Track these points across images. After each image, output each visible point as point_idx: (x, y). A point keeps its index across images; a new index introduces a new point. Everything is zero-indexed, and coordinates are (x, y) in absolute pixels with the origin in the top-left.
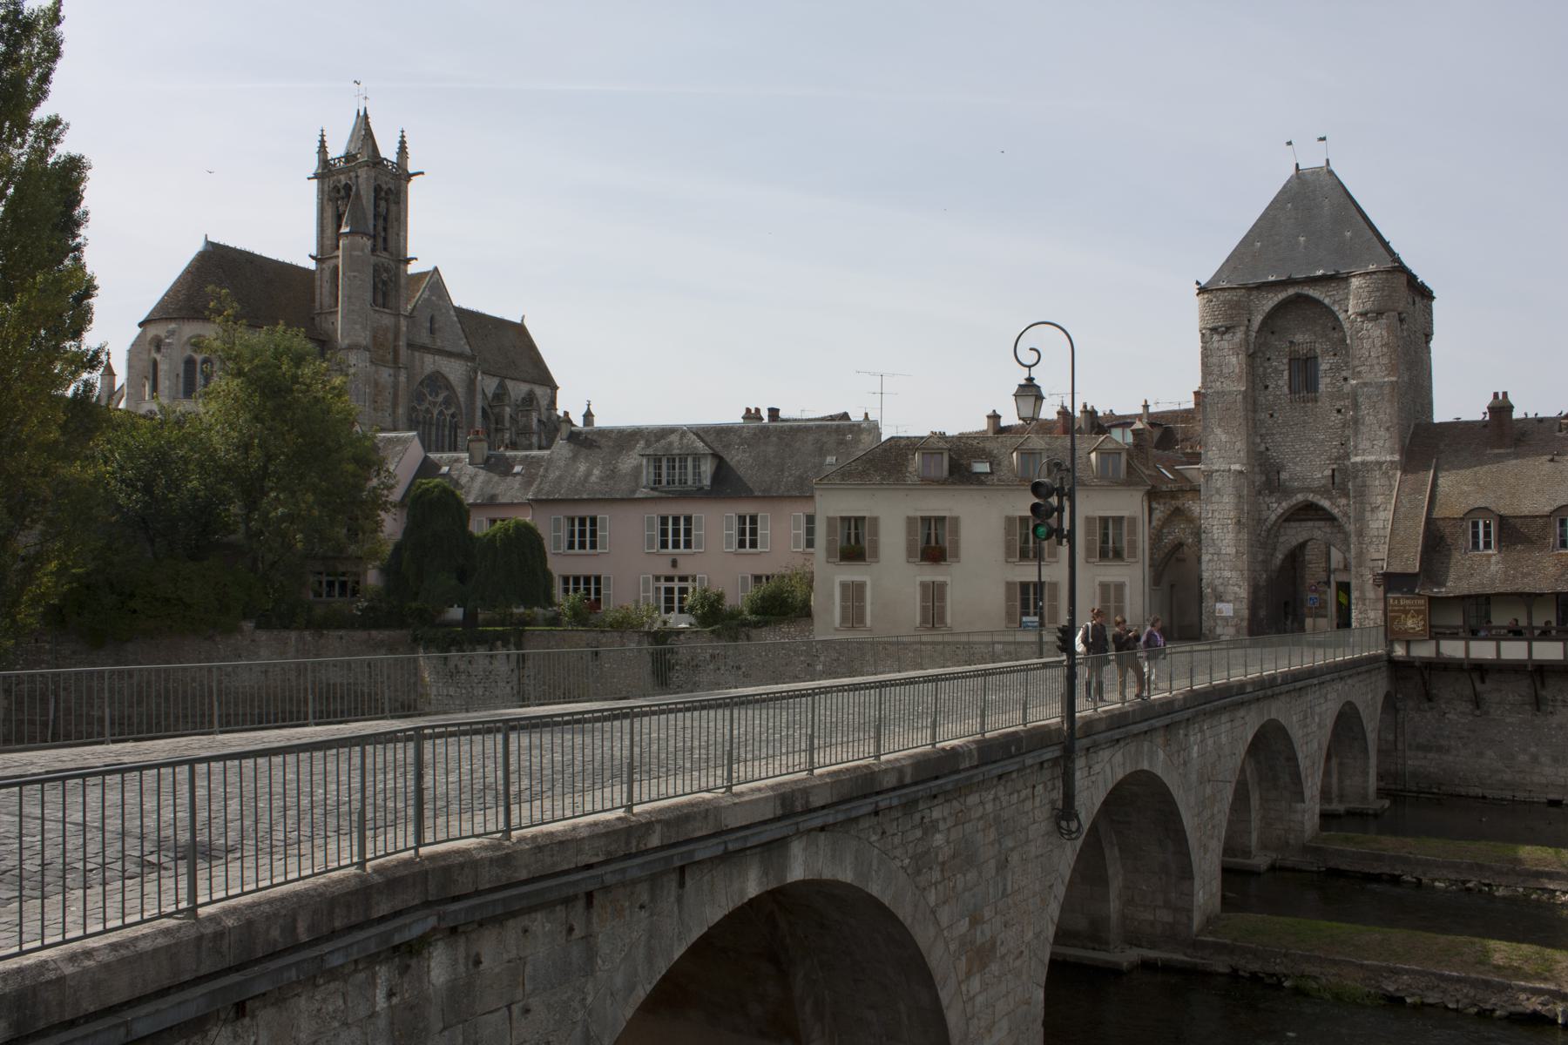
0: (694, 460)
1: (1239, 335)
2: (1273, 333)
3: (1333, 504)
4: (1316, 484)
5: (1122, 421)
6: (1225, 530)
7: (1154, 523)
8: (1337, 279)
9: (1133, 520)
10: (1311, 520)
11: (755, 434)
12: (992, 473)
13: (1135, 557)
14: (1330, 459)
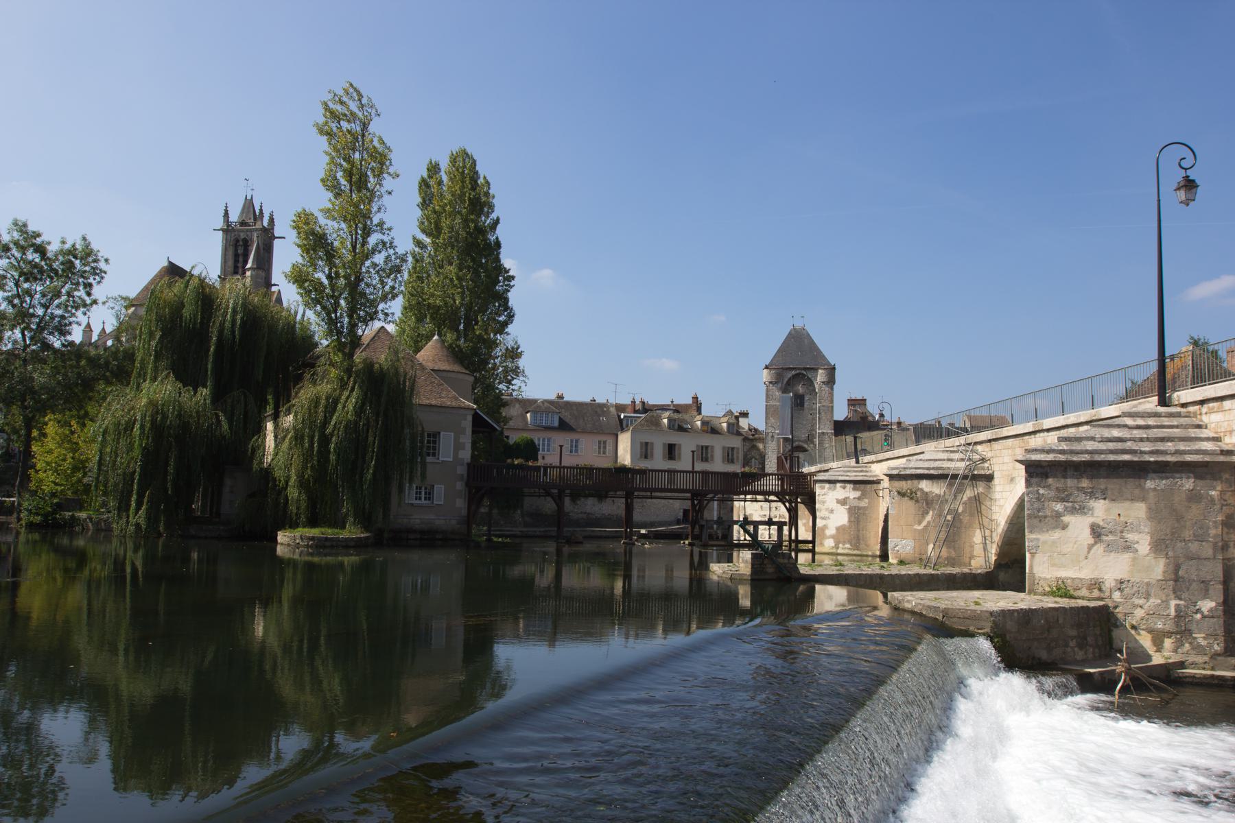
1: (780, 385)
8: (816, 370)
9: (738, 449)
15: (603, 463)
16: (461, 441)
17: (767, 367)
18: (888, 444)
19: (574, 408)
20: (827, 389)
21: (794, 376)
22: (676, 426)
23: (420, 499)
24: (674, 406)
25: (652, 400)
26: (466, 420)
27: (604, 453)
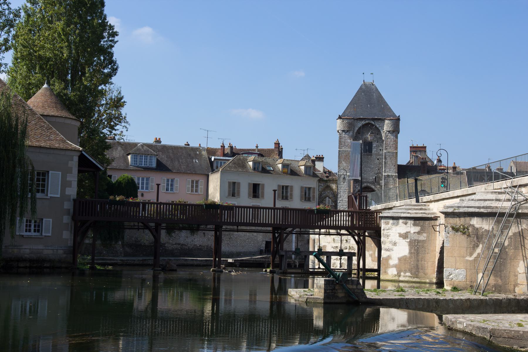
0: (150, 157)
1: (351, 133)
2: (359, 133)
3: (375, 187)
4: (370, 181)
5: (248, 152)
6: (345, 193)
7: (320, 190)
8: (382, 120)
9: (314, 189)
10: (366, 192)
11: (162, 148)
12: (273, 170)
13: (314, 200)
14: (375, 173)
15: (196, 200)
16: (68, 179)
17: (340, 117)
18: (444, 186)
19: (171, 151)
20: (392, 137)
21: (364, 126)
22: (260, 169)
23: (30, 231)
24: (259, 150)
25: (239, 146)
26: (72, 160)
27: (196, 191)
